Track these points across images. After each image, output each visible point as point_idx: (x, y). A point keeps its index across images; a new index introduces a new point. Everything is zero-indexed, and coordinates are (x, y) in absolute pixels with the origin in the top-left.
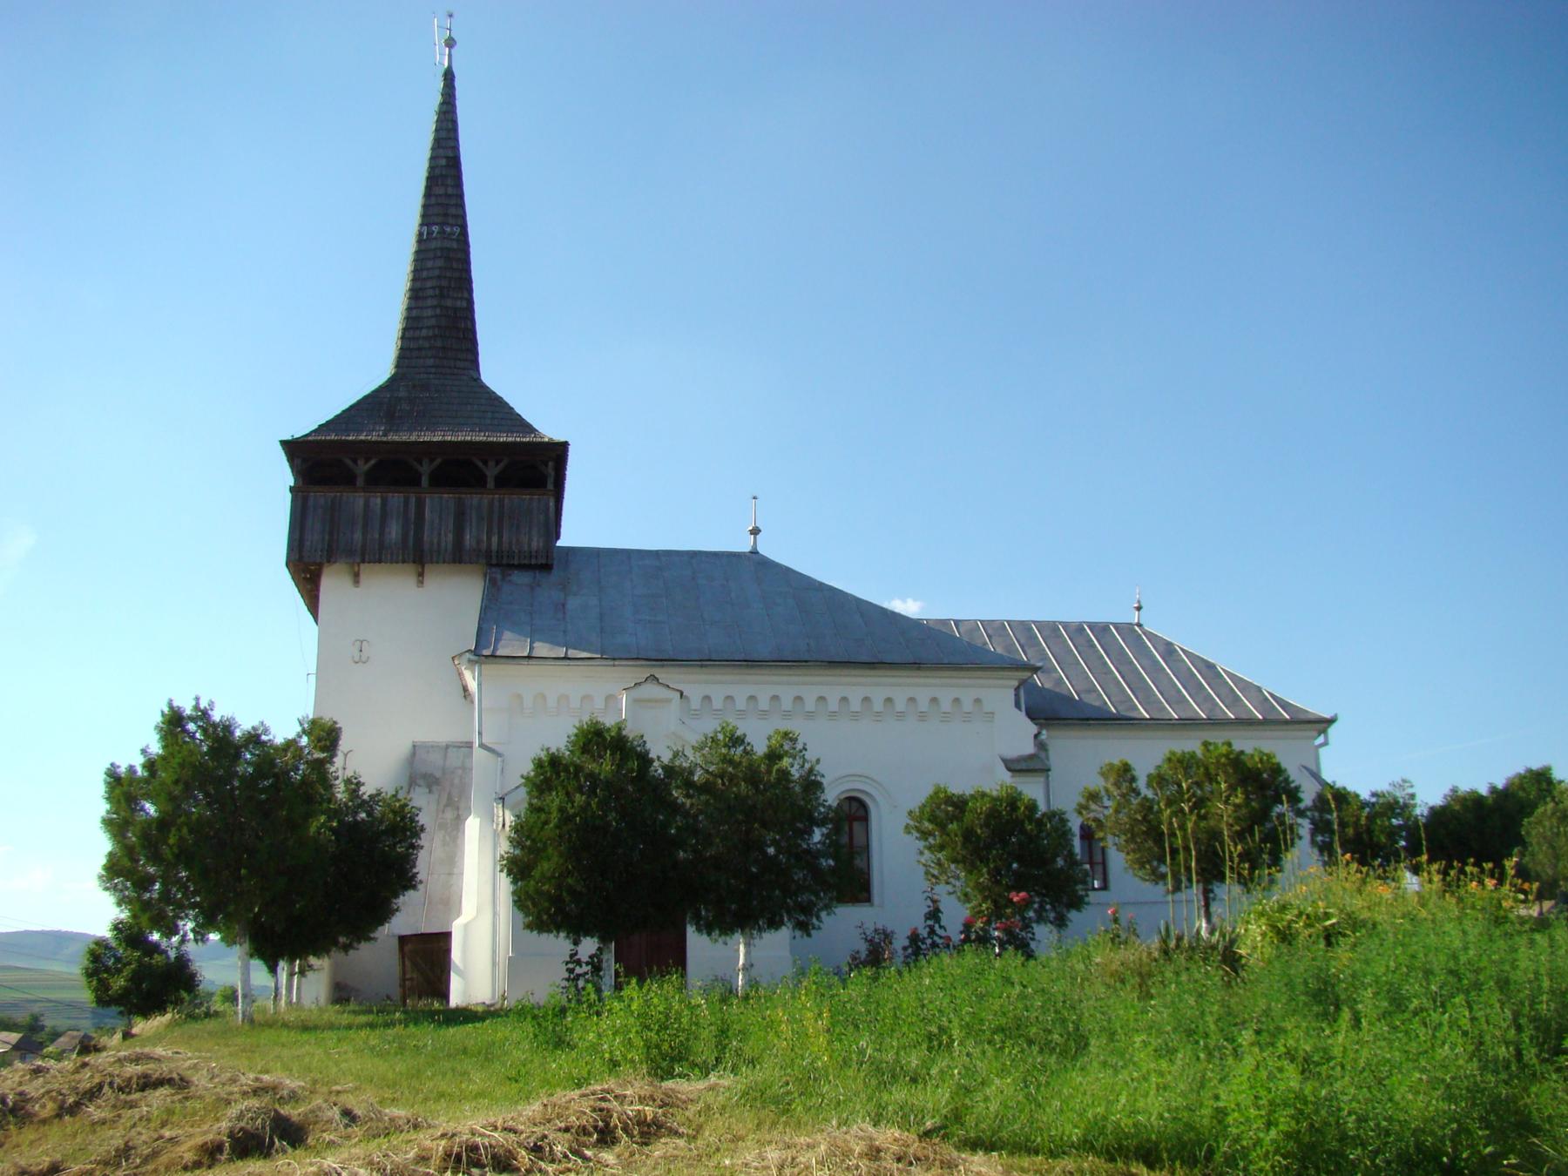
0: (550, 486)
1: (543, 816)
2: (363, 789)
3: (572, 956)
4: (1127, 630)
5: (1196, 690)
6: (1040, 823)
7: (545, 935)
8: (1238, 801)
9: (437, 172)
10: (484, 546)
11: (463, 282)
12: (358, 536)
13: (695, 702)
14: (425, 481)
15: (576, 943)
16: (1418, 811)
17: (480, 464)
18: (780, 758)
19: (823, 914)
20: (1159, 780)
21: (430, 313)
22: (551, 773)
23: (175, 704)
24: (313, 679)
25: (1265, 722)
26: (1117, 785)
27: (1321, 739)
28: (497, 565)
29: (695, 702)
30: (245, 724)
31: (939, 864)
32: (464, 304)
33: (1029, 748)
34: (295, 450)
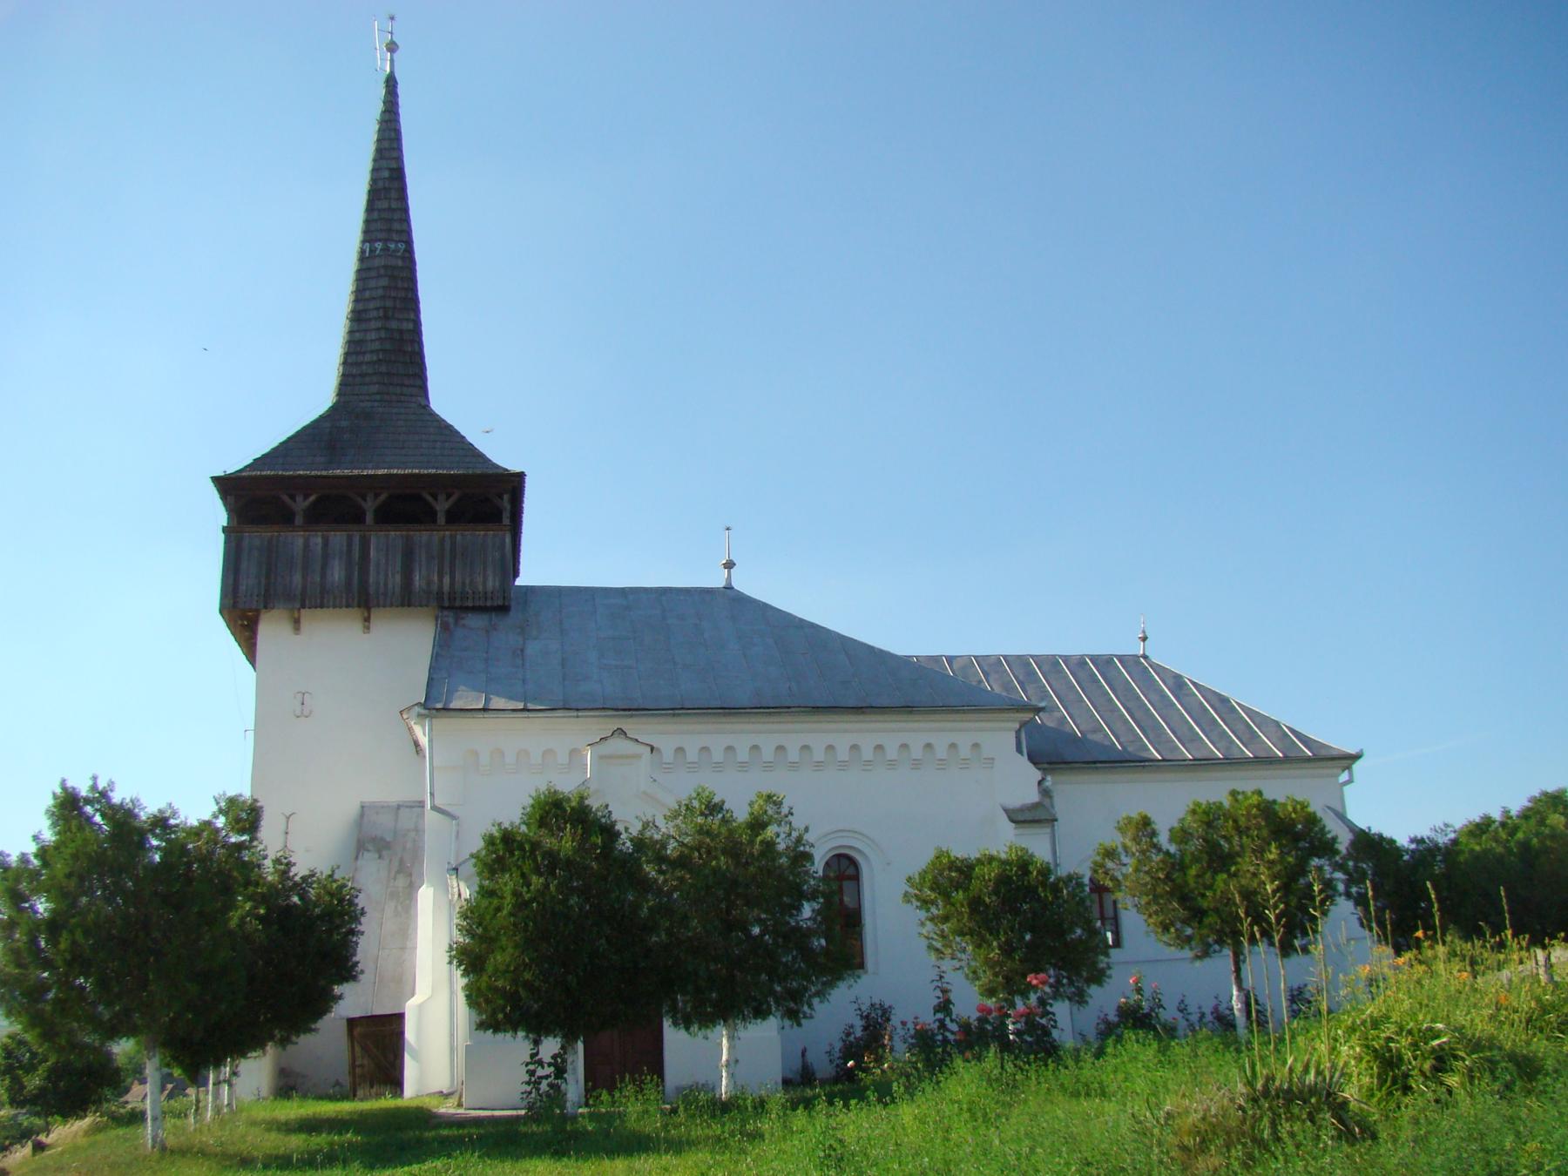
0: (506, 521)
1: (496, 902)
2: (294, 870)
3: (532, 1056)
4: (1133, 663)
5: (1209, 726)
6: (1055, 888)
7: (500, 1036)
8: (1272, 857)
9: (380, 184)
10: (435, 588)
11: (410, 303)
12: (298, 578)
13: (668, 755)
14: (369, 518)
15: (537, 1043)
16: (1461, 858)
17: (430, 499)
18: (764, 826)
19: (816, 1001)
20: (1181, 835)
21: (373, 336)
22: (503, 852)
23: (69, 784)
24: (251, 735)
25: (1287, 760)
26: (1136, 840)
27: (1344, 777)
28: (450, 608)
29: (668, 755)
30: (150, 806)
31: (943, 936)
32: (411, 326)
33: (1033, 796)
34: (227, 486)
